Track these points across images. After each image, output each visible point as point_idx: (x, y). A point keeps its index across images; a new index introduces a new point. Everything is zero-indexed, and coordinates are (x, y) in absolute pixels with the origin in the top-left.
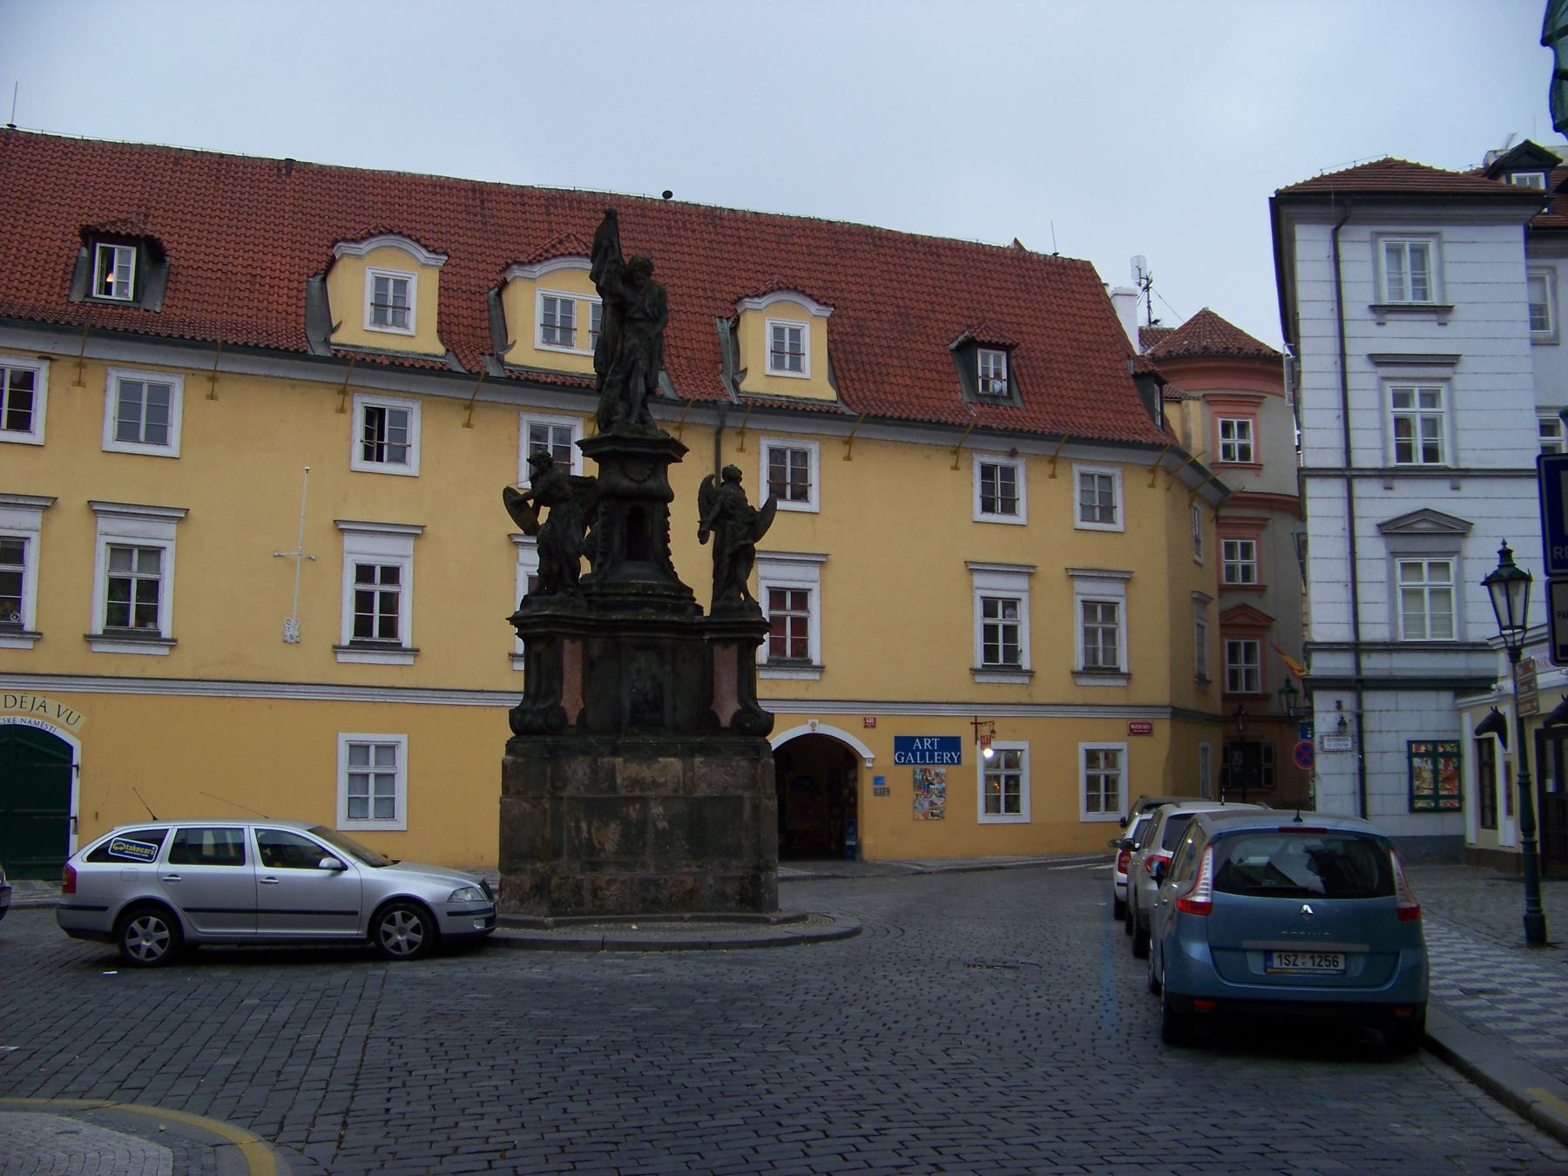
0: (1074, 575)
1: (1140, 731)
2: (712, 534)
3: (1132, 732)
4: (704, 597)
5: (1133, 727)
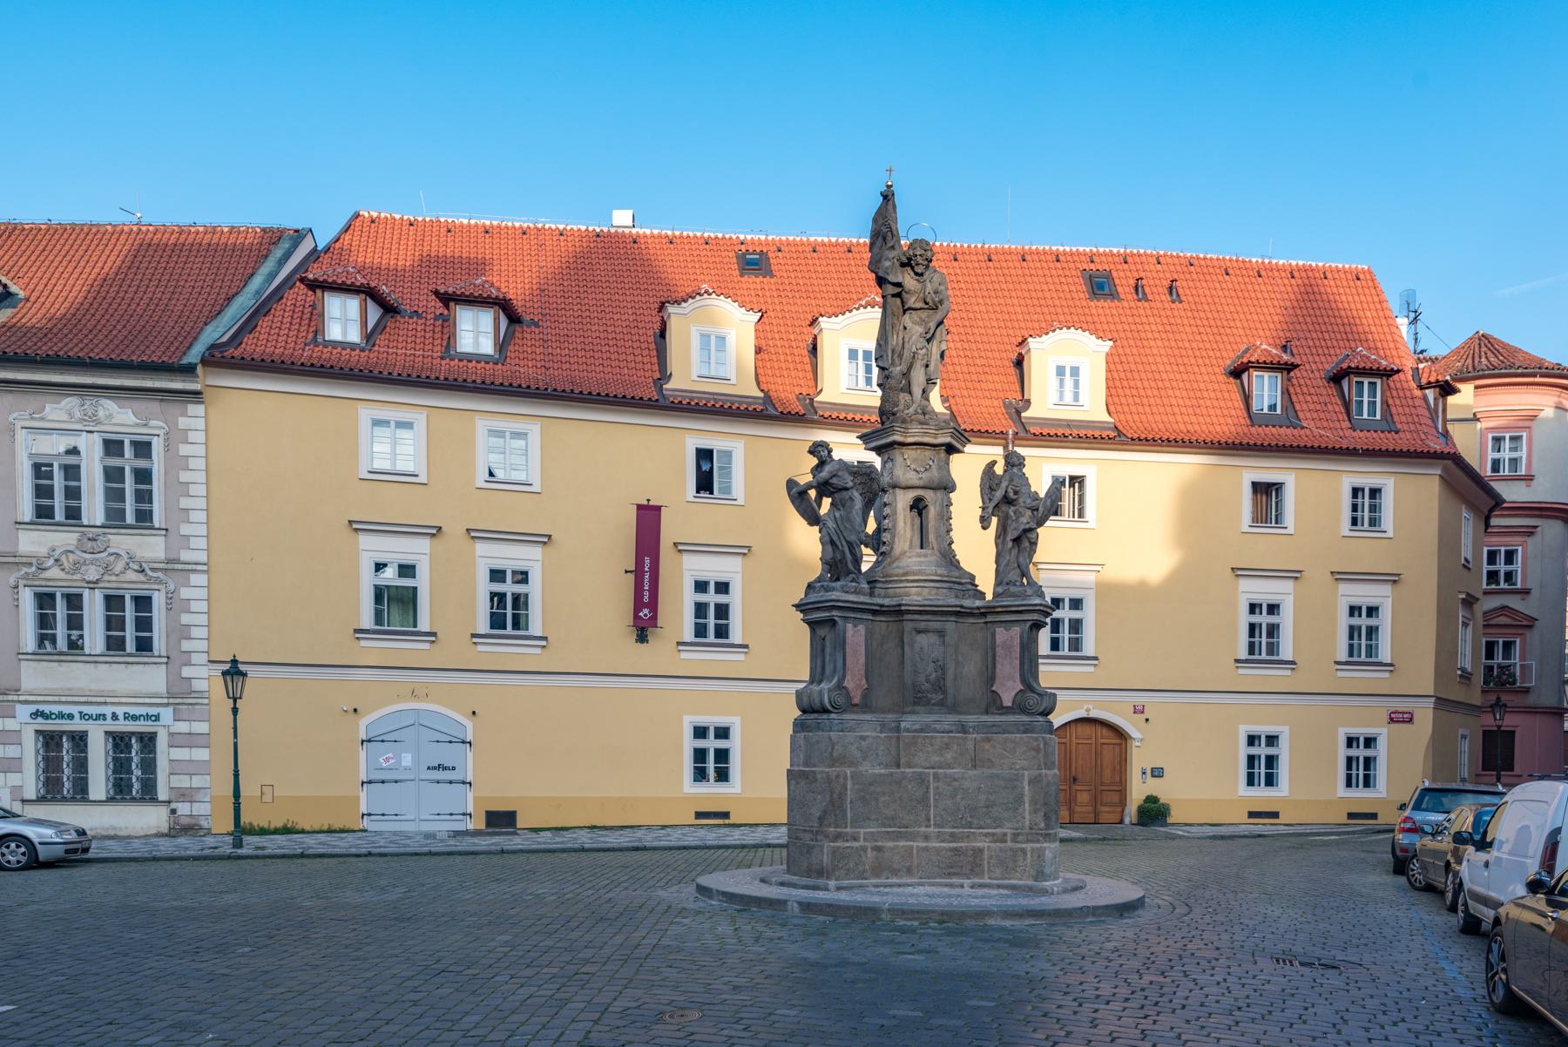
0: (1340, 576)
1: (1400, 718)
2: (995, 520)
3: (1392, 720)
4: (986, 583)
5: (1393, 716)
